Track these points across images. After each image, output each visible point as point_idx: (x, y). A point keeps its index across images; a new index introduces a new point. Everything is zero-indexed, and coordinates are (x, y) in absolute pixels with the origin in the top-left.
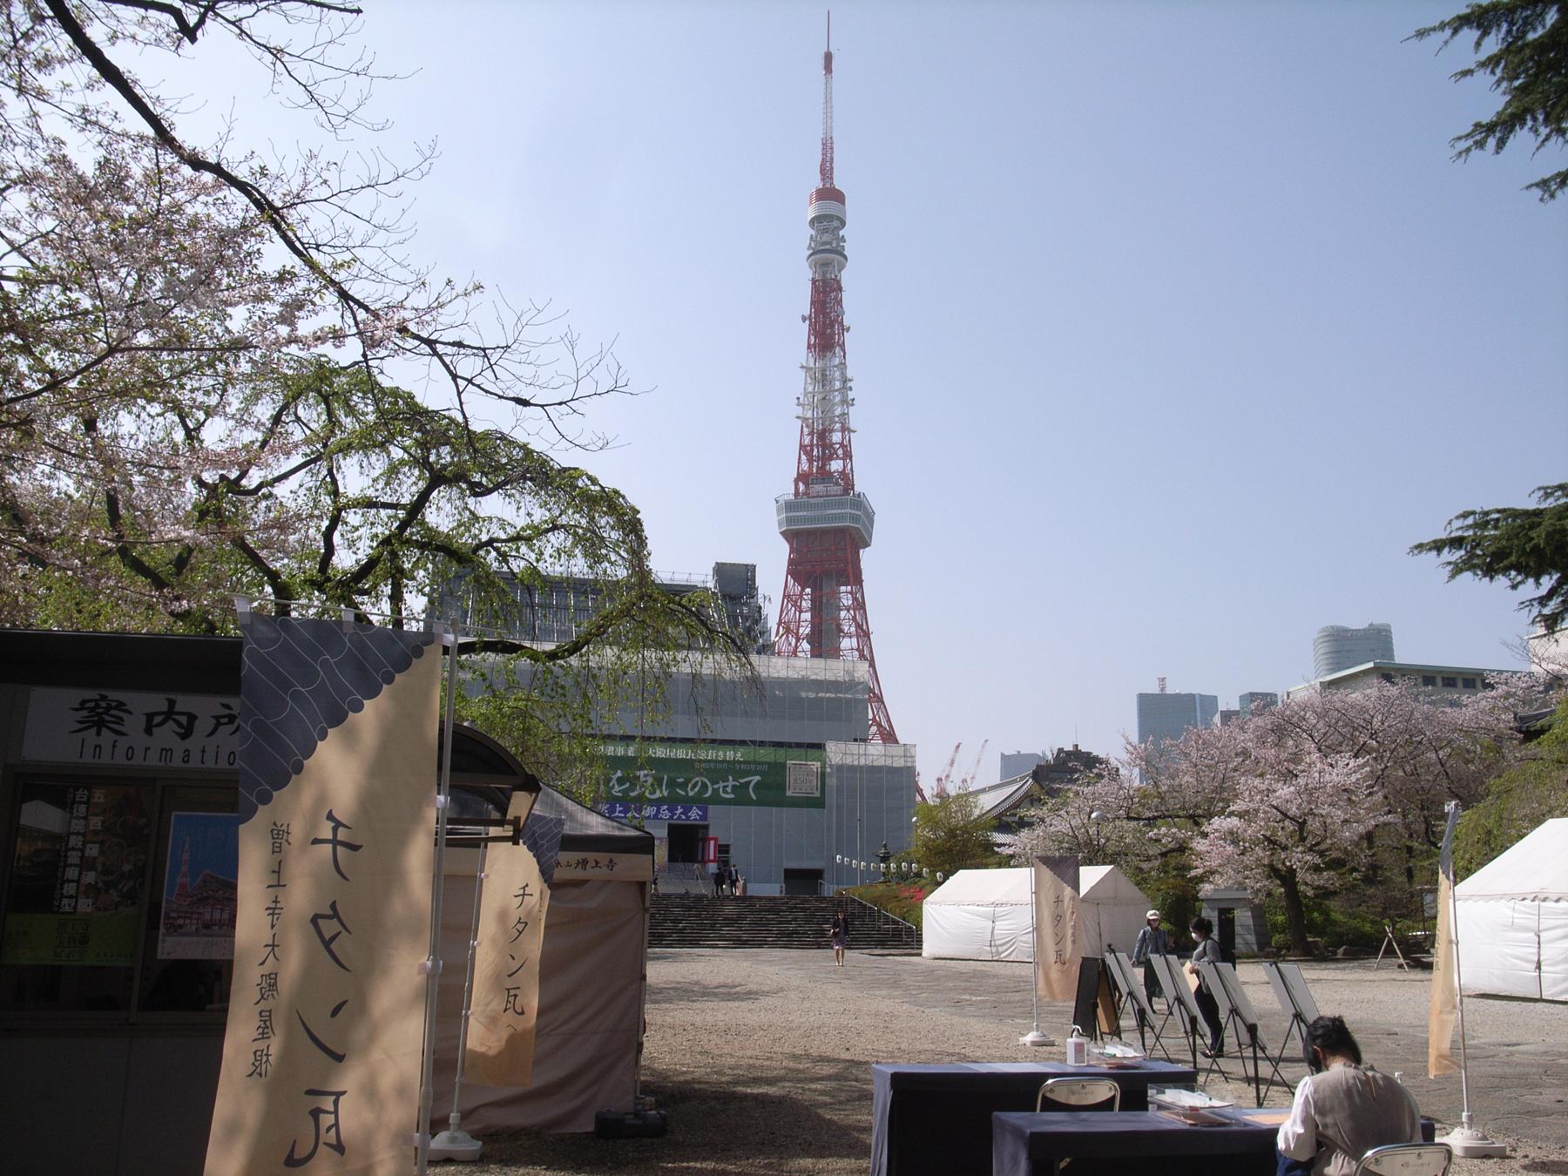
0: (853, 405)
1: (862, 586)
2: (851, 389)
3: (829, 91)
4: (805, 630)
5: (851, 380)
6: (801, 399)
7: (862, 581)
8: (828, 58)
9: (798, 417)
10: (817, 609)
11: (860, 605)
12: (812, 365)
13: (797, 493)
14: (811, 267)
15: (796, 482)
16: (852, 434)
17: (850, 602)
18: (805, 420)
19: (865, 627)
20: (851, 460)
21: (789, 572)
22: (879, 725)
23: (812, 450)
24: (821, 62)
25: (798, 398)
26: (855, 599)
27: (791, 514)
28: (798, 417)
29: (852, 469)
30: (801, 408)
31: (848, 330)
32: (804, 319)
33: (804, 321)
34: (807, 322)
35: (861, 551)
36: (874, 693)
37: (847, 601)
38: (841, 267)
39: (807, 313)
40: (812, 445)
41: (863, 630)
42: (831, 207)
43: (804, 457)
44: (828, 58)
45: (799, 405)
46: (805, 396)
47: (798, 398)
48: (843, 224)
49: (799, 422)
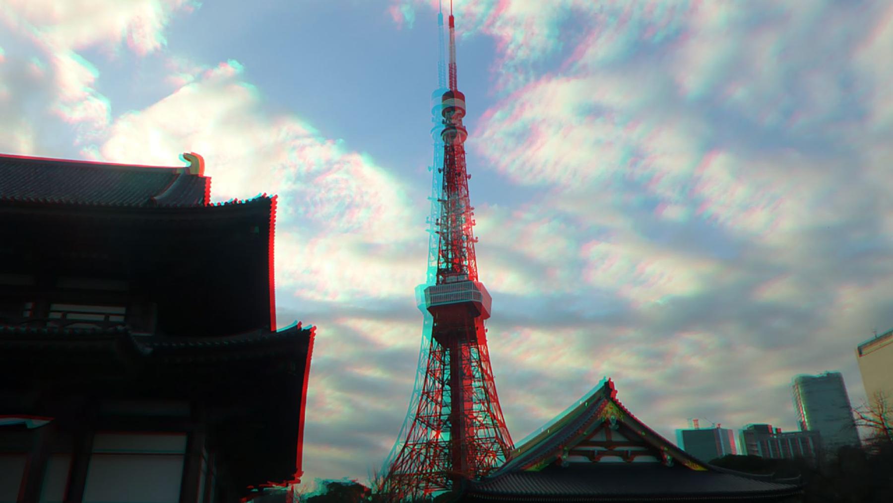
0: (474, 225)
1: (486, 345)
2: (473, 214)
5: (473, 209)
6: (439, 222)
7: (486, 341)
9: (437, 232)
12: (446, 198)
15: (438, 276)
16: (475, 244)
18: (442, 234)
19: (489, 372)
20: (475, 260)
21: (433, 336)
22: (502, 442)
23: (448, 254)
28: (437, 232)
29: (475, 265)
30: (439, 227)
31: (470, 177)
32: (440, 171)
34: (442, 173)
35: (484, 321)
36: (498, 420)
38: (464, 138)
39: (442, 167)
40: (447, 250)
41: (488, 375)
42: (456, 102)
43: (442, 260)
45: (437, 224)
46: (442, 219)
48: (464, 113)
49: (439, 235)
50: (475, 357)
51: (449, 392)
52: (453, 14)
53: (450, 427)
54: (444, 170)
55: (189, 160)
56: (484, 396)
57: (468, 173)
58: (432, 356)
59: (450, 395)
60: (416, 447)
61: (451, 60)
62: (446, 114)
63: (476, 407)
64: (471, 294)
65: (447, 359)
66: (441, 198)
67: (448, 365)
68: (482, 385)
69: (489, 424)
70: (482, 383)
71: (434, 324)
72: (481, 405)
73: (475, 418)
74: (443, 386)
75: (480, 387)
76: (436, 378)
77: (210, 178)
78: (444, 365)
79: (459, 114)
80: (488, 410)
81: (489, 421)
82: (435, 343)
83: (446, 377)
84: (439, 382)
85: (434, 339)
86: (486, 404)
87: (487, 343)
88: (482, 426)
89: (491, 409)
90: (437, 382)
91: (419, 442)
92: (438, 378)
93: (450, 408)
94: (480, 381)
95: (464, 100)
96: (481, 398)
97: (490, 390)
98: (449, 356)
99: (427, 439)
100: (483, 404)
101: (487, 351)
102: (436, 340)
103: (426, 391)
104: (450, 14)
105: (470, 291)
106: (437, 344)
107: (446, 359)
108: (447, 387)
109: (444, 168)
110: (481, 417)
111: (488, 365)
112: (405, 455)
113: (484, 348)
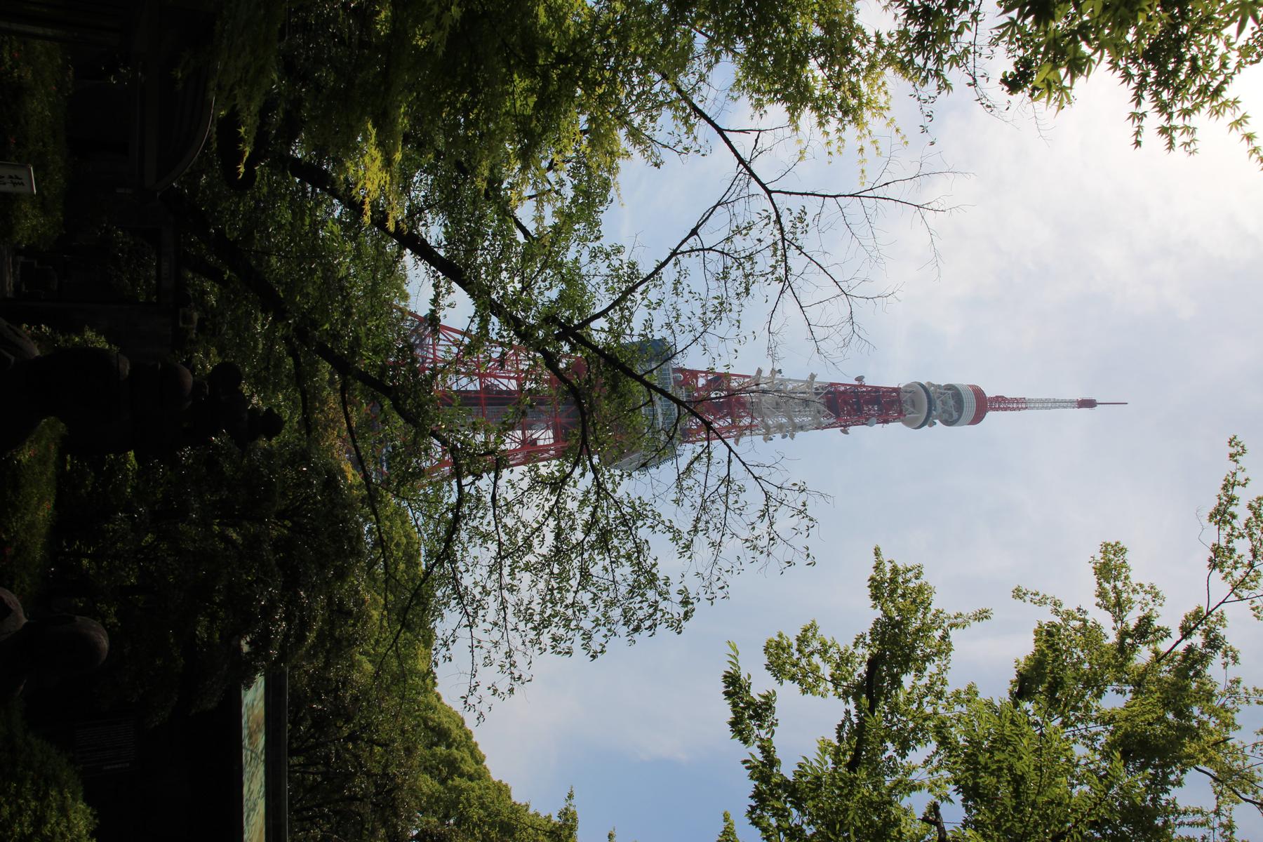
0: (765, 440)
2: (784, 437)
3: (1065, 404)
6: (778, 376)
8: (1088, 404)
9: (759, 371)
14: (906, 386)
24: (1087, 397)
25: (780, 371)
28: (759, 371)
31: (845, 432)
32: (859, 379)
33: (857, 379)
34: (856, 383)
38: (909, 423)
42: (970, 406)
44: (1088, 404)
47: (780, 371)
48: (948, 423)
49: (753, 374)
54: (861, 386)
57: (852, 429)
61: (1030, 401)
62: (950, 392)
66: (816, 380)
79: (951, 415)
109: (864, 386)
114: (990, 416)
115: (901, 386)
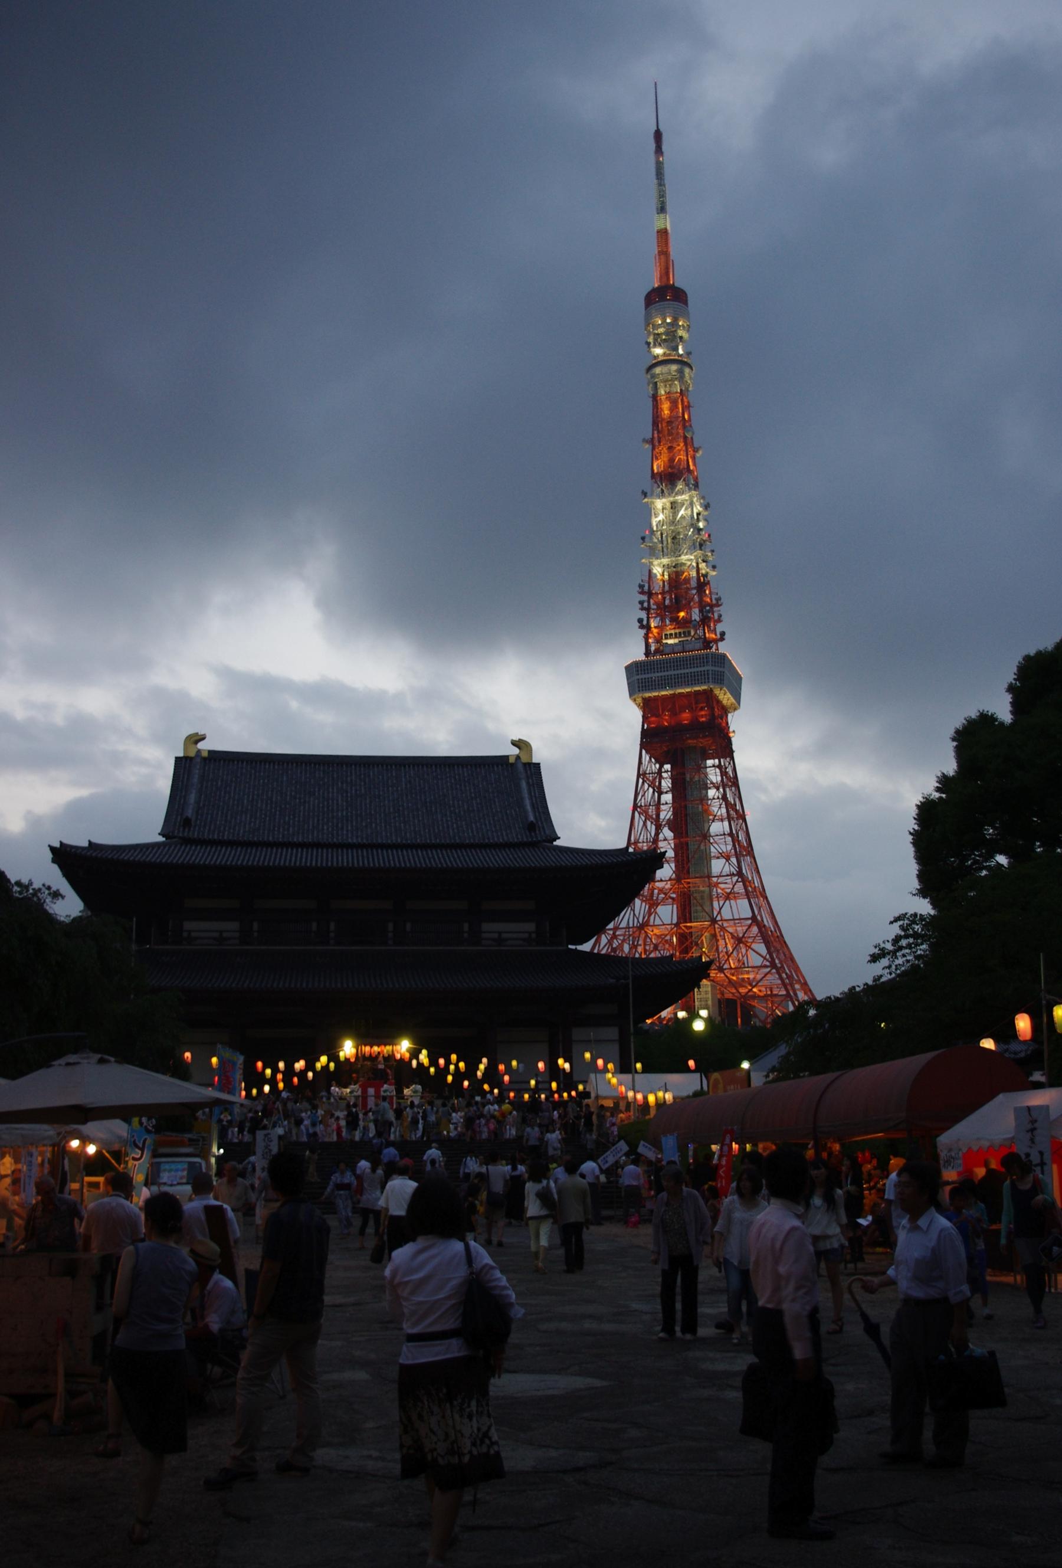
1: (732, 758)
4: (666, 814)
8: (658, 136)
10: (679, 788)
11: (731, 781)
13: (647, 653)
17: (719, 778)
21: (643, 746)
22: (761, 926)
23: (664, 599)
26: (724, 773)
27: (643, 676)
35: (730, 716)
37: (714, 776)
39: (649, 436)
40: (663, 593)
41: (737, 811)
44: (658, 136)
50: (715, 781)
51: (672, 842)
52: (660, 127)
53: (673, 899)
55: (519, 748)
56: (729, 847)
57: (696, 445)
58: (641, 781)
59: (673, 847)
60: (617, 933)
63: (718, 866)
64: (708, 674)
65: (666, 784)
67: (666, 793)
68: (727, 830)
69: (738, 893)
70: (726, 823)
71: (643, 726)
72: (724, 860)
73: (717, 885)
74: (659, 828)
75: (724, 834)
76: (648, 817)
77: (539, 764)
78: (660, 793)
80: (740, 873)
81: (739, 888)
82: (646, 757)
83: (662, 815)
84: (652, 823)
85: (644, 752)
86: (734, 860)
87: (735, 755)
88: (728, 896)
89: (744, 871)
90: (649, 823)
91: (621, 926)
92: (651, 817)
93: (673, 865)
94: (722, 820)
95: (686, 303)
96: (725, 850)
97: (742, 836)
98: (670, 781)
99: (638, 921)
100: (728, 859)
101: (734, 770)
102: (647, 752)
103: (632, 839)
104: (656, 129)
105: (706, 668)
106: (648, 758)
107: (663, 783)
108: (667, 833)
109: (653, 438)
110: (726, 883)
111: (737, 795)
112: (601, 948)
113: (730, 763)
114: (679, 279)
115: (651, 395)
